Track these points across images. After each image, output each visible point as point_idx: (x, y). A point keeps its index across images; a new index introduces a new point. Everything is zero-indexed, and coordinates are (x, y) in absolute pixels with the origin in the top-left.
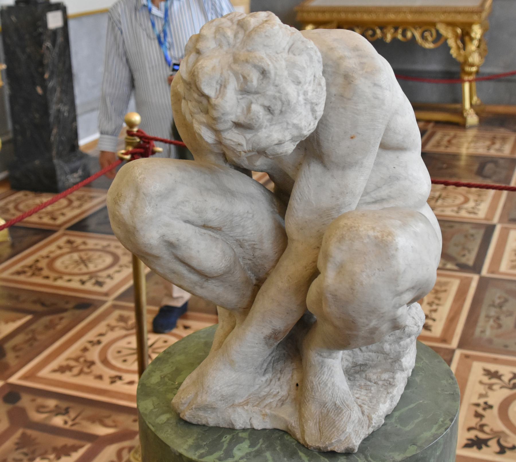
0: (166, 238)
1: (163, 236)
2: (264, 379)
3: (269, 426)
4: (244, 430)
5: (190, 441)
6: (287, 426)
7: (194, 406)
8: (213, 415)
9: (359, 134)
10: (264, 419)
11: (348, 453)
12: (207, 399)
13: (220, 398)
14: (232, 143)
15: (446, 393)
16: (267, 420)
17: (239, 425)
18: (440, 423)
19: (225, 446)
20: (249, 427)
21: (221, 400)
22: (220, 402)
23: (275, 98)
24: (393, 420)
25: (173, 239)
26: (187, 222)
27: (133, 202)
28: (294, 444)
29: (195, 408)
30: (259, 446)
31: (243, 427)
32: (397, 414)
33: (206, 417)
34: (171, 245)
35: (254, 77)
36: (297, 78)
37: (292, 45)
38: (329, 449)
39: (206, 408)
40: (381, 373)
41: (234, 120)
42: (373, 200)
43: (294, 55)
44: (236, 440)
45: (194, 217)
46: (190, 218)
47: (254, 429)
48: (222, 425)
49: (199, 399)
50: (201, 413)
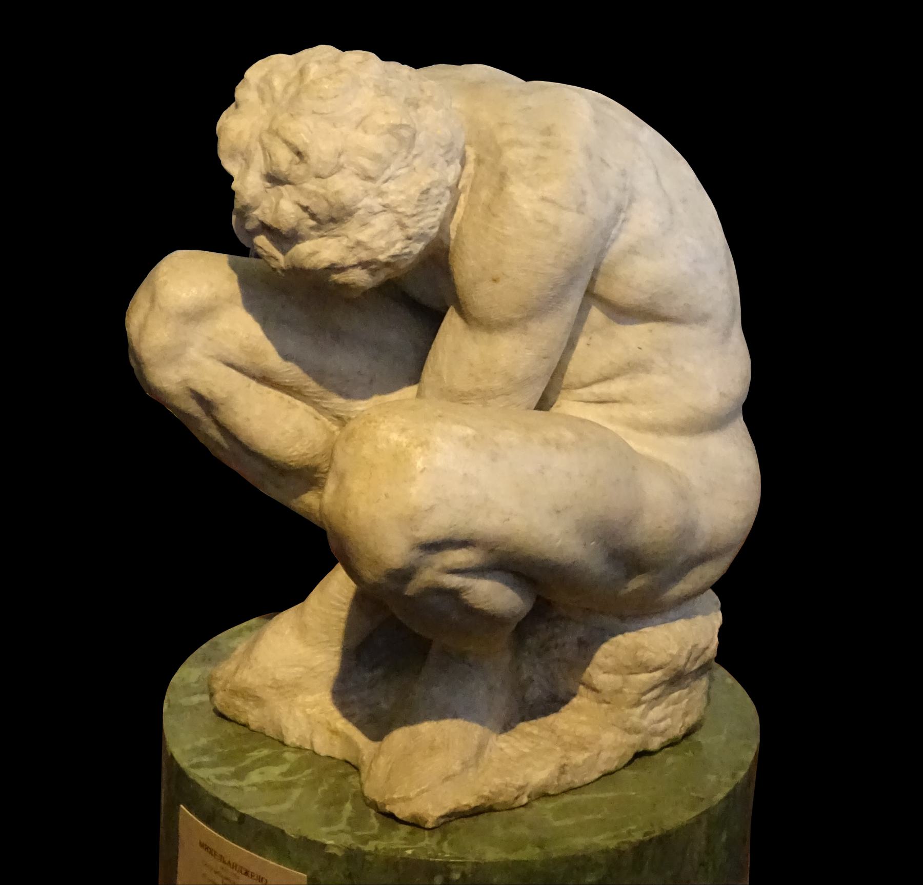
0: (192, 386)
1: (186, 381)
2: (368, 675)
3: (338, 753)
4: (299, 749)
5: (203, 741)
6: (357, 759)
7: (228, 686)
8: (256, 712)
9: (508, 277)
10: (331, 738)
11: (416, 824)
12: (248, 677)
13: (269, 683)
14: (264, 254)
15: (693, 794)
16: (337, 742)
17: (292, 738)
18: (624, 831)
19: (247, 762)
20: (308, 747)
21: (271, 687)
22: (268, 690)
23: (316, 194)
24: (550, 805)
25: (202, 390)
26: (231, 365)
27: (146, 318)
28: (354, 790)
29: (231, 690)
30: (296, 777)
31: (298, 744)
32: (567, 798)
33: (245, 712)
34: (200, 399)
35: (283, 157)
36: (364, 170)
37: (367, 116)
38: (388, 808)
39: (246, 694)
40: (581, 723)
41: (261, 218)
42: (596, 399)
43: (366, 132)
44: (275, 760)
45: (242, 361)
46: (232, 359)
47: (314, 752)
48: (270, 732)
49: (238, 676)
50: (238, 702)
